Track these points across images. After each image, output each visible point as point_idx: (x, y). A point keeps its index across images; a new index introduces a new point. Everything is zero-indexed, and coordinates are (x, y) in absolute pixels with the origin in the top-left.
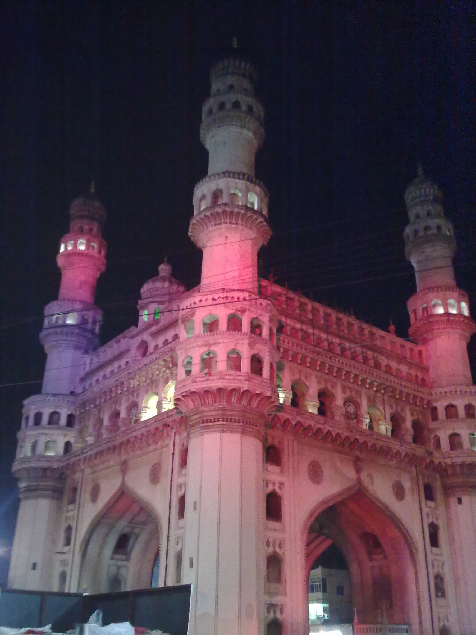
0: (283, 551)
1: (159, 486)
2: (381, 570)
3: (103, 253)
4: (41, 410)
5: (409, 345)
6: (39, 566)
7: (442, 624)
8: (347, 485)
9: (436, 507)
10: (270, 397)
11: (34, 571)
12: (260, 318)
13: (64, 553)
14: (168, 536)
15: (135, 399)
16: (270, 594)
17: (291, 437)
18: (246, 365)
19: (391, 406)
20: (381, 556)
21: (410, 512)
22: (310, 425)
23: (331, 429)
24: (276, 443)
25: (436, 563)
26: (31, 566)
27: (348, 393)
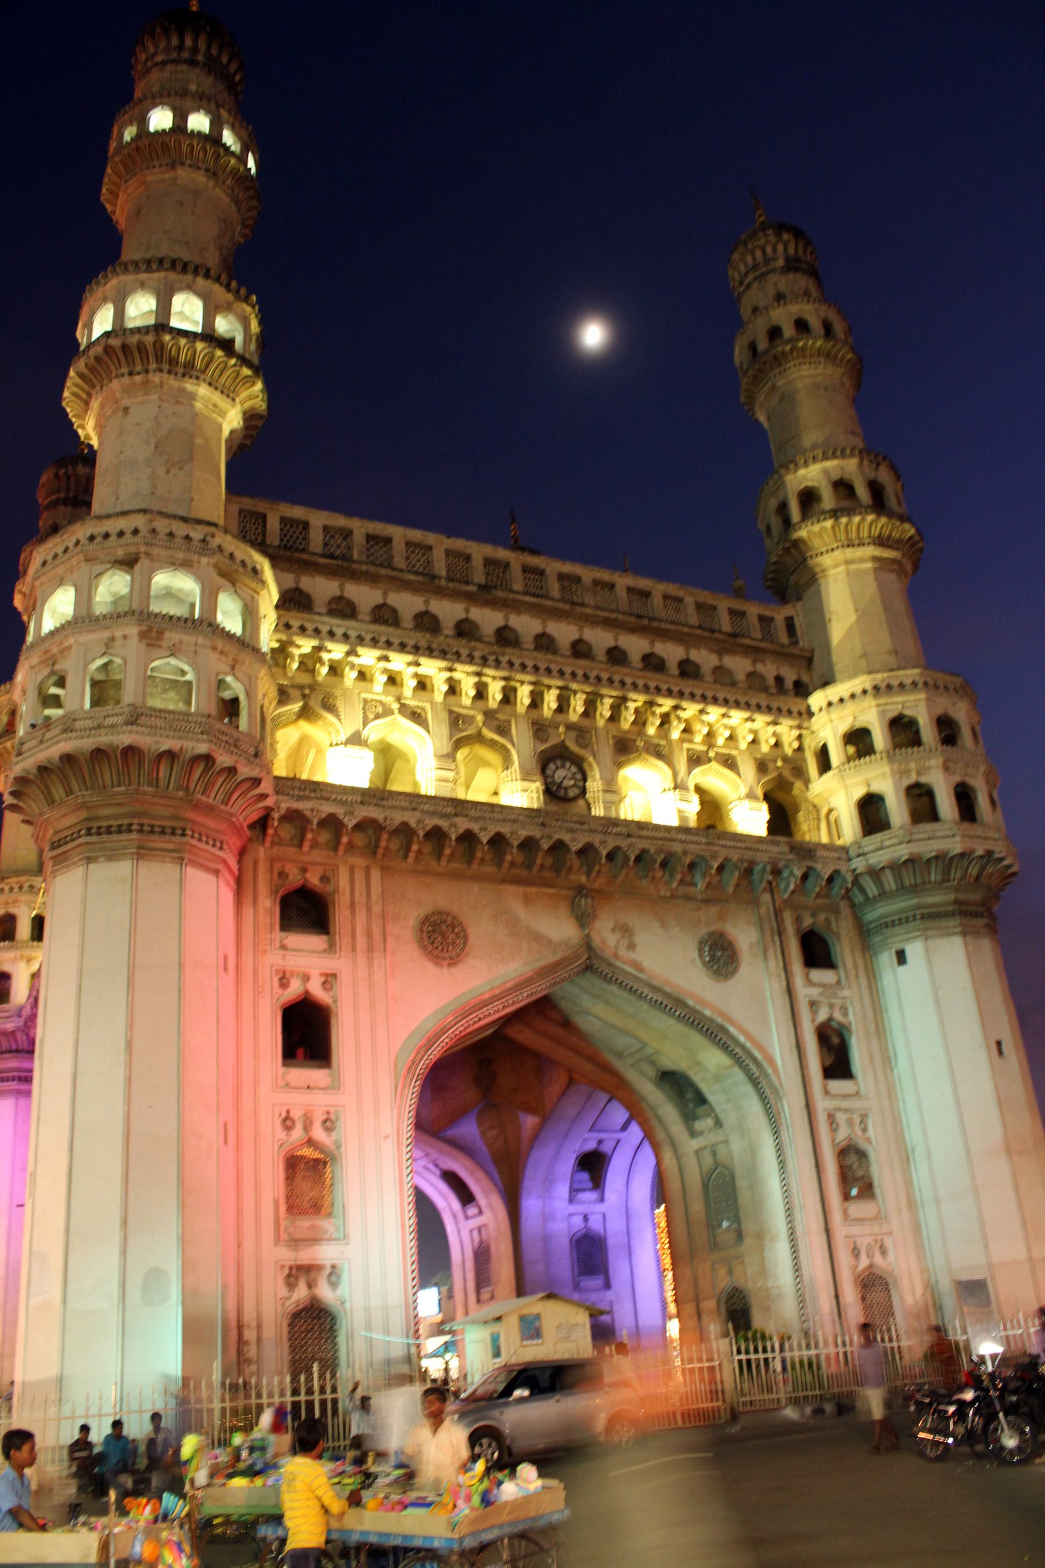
2: (714, 1154)
7: (864, 1262)
8: (550, 959)
9: (838, 982)
16: (295, 1242)
17: (360, 862)
20: (710, 1122)
22: (405, 824)
23: (475, 827)
24: (314, 879)
25: (841, 1118)
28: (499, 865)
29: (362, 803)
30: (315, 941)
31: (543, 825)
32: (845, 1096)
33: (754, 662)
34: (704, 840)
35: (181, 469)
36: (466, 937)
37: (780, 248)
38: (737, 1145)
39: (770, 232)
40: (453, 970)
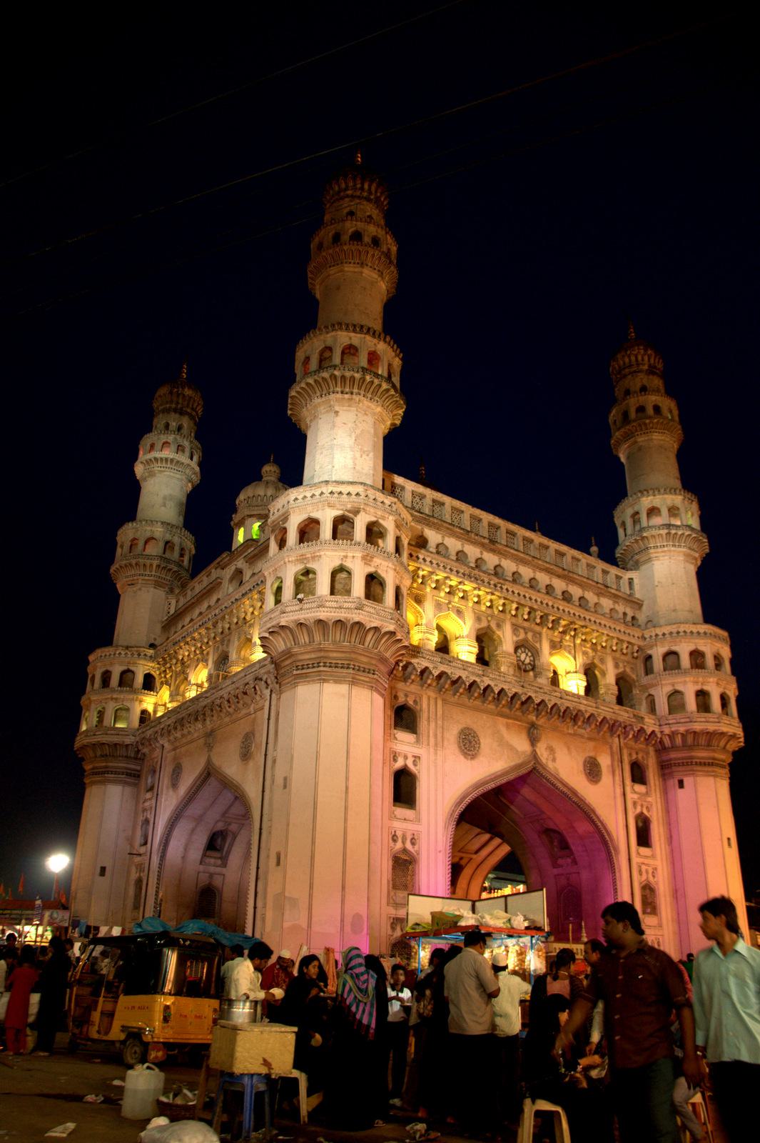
0: (416, 847)
1: (251, 764)
3: (195, 458)
5: (614, 571)
6: (108, 873)
8: (518, 761)
10: (393, 633)
11: (101, 878)
12: (381, 521)
13: (140, 855)
15: (225, 649)
16: (397, 905)
17: (432, 695)
18: (358, 587)
20: (569, 860)
21: (609, 801)
22: (460, 677)
23: (492, 684)
24: (411, 702)
25: (644, 868)
26: (98, 870)
27: (522, 636)
28: (497, 706)
29: (440, 662)
31: (523, 686)
32: (646, 857)
34: (594, 705)
35: (368, 455)
36: (479, 744)
37: (646, 358)
38: (585, 875)
39: (642, 348)
40: (473, 762)
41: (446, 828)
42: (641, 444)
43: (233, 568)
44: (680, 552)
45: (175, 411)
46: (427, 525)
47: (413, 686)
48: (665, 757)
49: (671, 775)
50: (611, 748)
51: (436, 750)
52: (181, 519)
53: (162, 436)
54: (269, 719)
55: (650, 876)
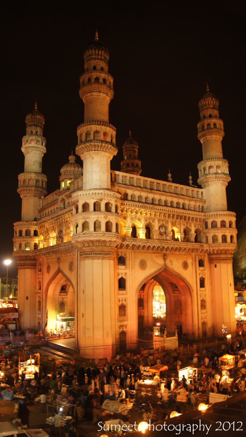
0: (126, 302)
1: (73, 273)
2: (178, 297)
3: (44, 144)
4: (22, 229)
6: (29, 298)
8: (159, 267)
14: (77, 296)
17: (130, 251)
19: (184, 225)
20: (178, 292)
21: (190, 275)
23: (150, 245)
24: (123, 255)
26: (26, 298)
27: (161, 223)
30: (123, 267)
31: (161, 243)
33: (196, 202)
34: (186, 245)
35: (105, 174)
36: (146, 264)
37: (212, 102)
39: (211, 98)
41: (136, 294)
42: (208, 139)
43: (61, 197)
44: (220, 182)
45: (34, 125)
46: (128, 188)
47: (124, 250)
48: (211, 257)
49: (213, 263)
50: (192, 257)
51: (132, 270)
52: (41, 169)
53: (30, 137)
54: (77, 260)
55: (204, 297)
